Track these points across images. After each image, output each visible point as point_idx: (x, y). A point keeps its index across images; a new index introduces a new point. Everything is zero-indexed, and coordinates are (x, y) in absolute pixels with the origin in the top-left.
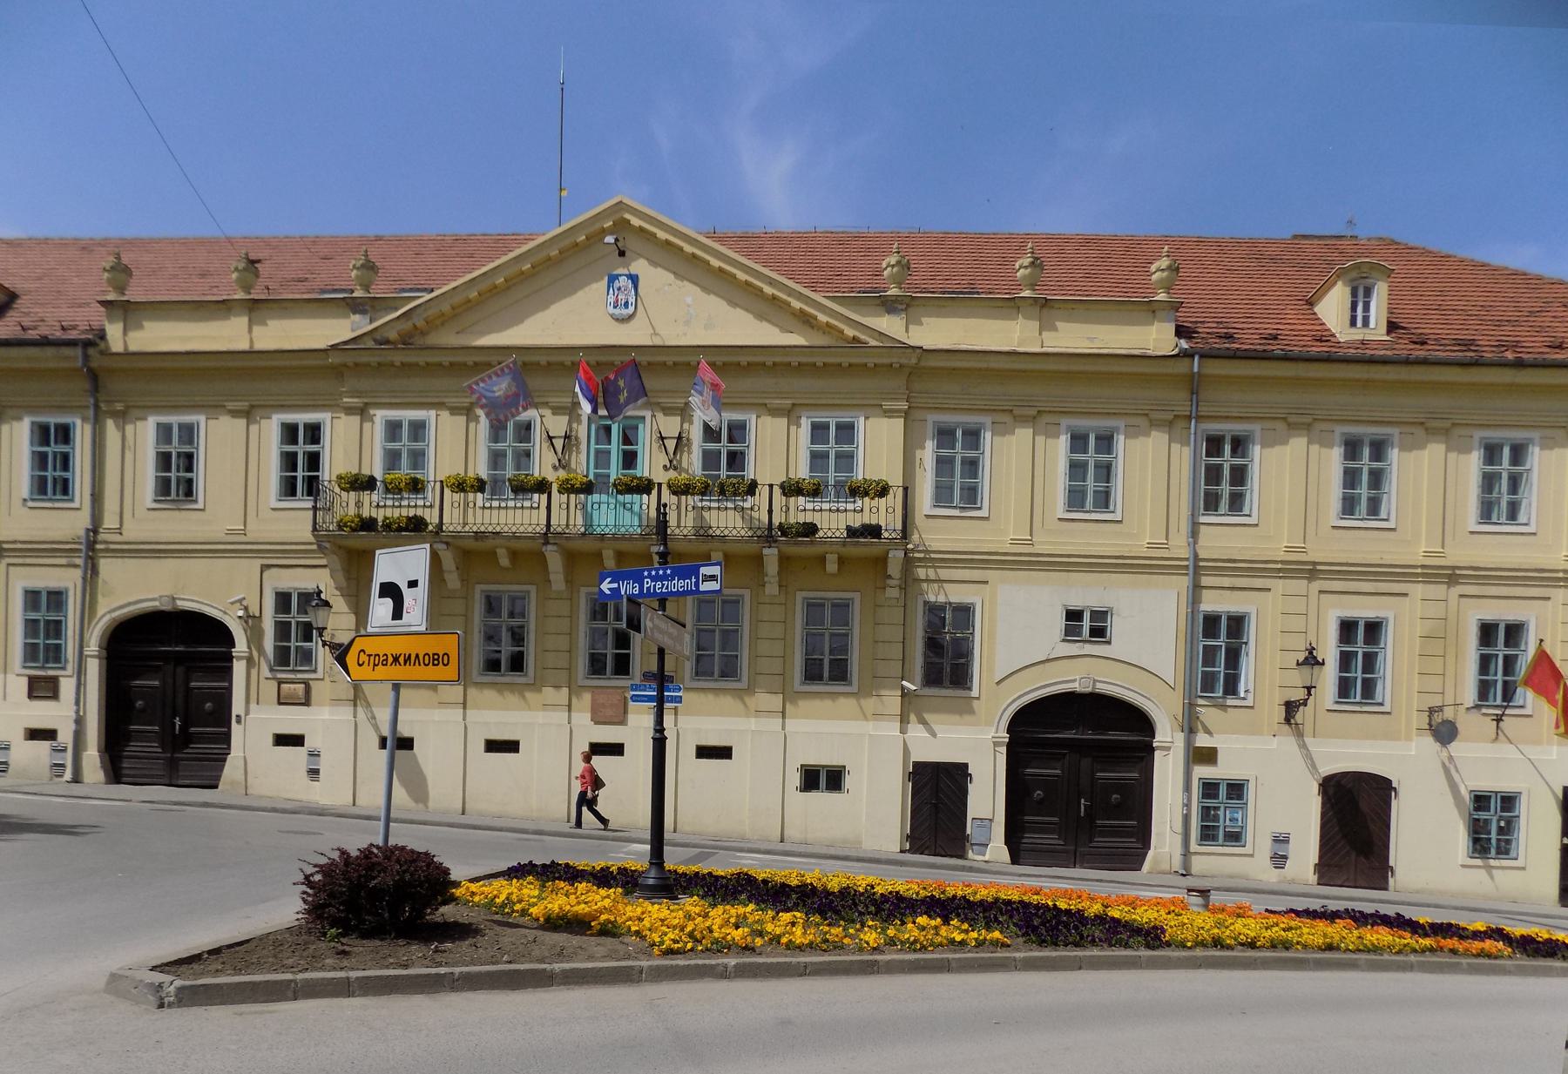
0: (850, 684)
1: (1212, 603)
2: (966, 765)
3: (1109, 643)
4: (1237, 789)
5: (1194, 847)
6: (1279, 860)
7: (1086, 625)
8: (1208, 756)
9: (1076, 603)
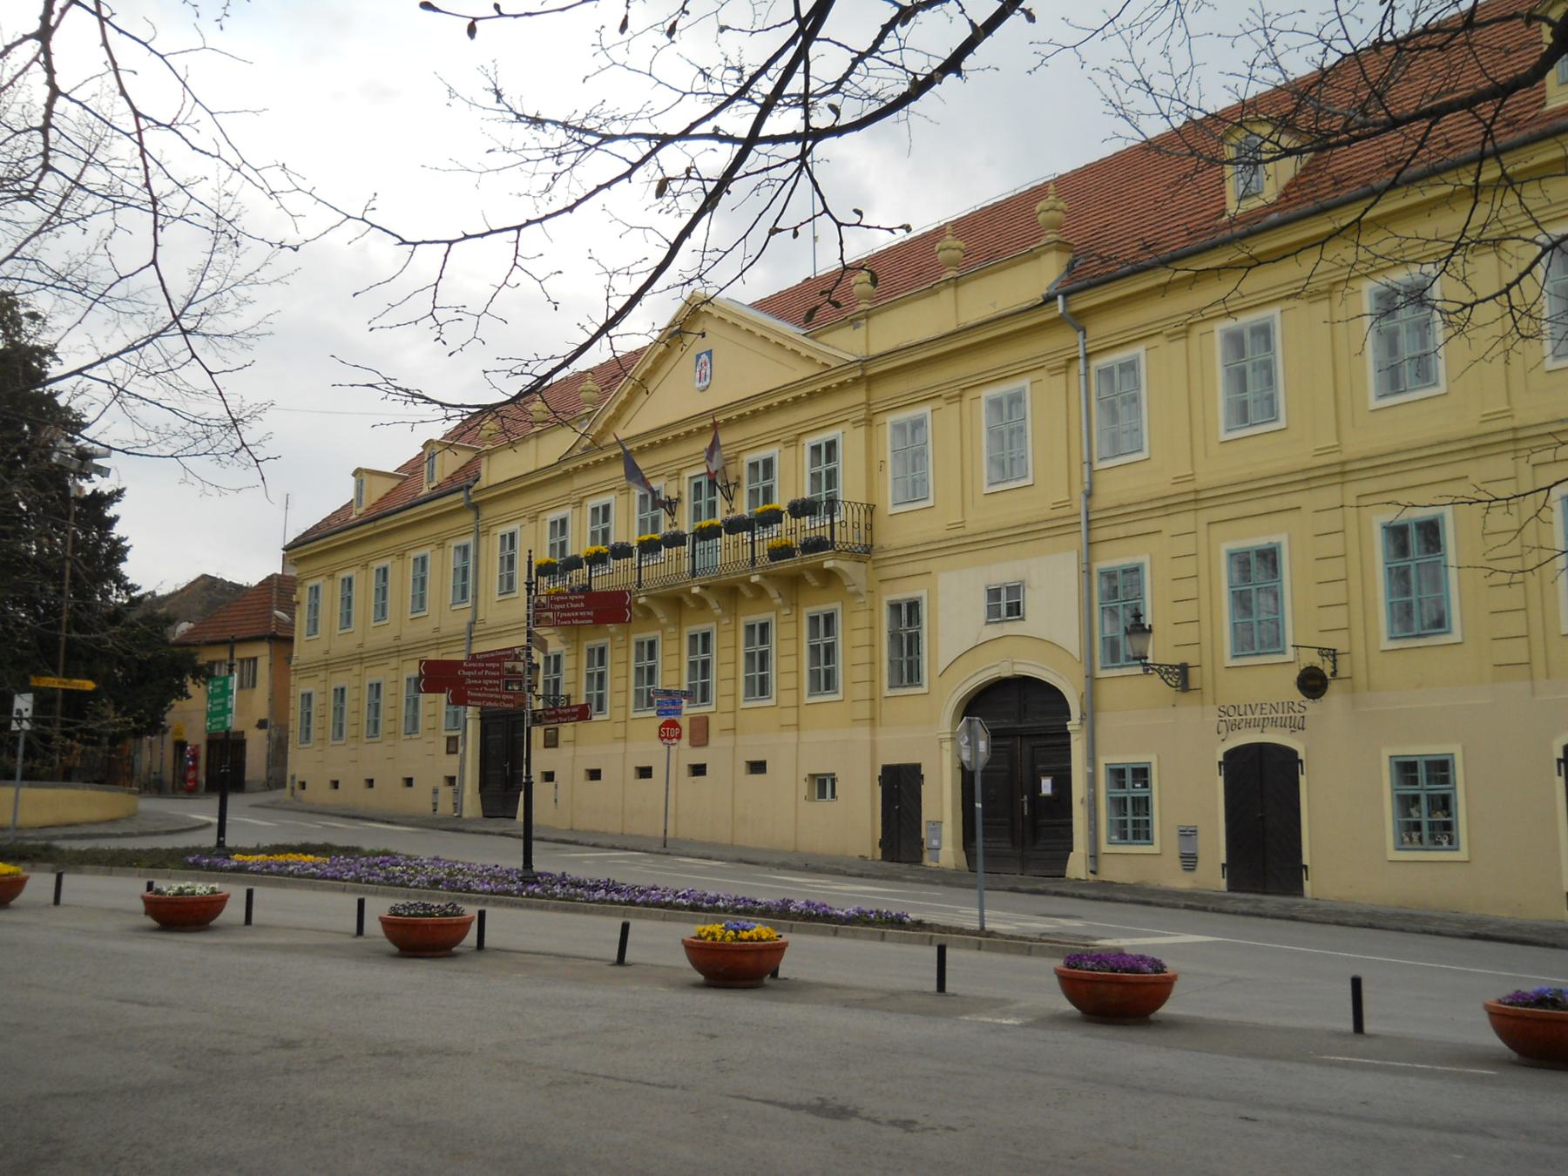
1: (1111, 558)
2: (917, 767)
5: (1104, 847)
6: (1189, 861)
7: (1007, 604)
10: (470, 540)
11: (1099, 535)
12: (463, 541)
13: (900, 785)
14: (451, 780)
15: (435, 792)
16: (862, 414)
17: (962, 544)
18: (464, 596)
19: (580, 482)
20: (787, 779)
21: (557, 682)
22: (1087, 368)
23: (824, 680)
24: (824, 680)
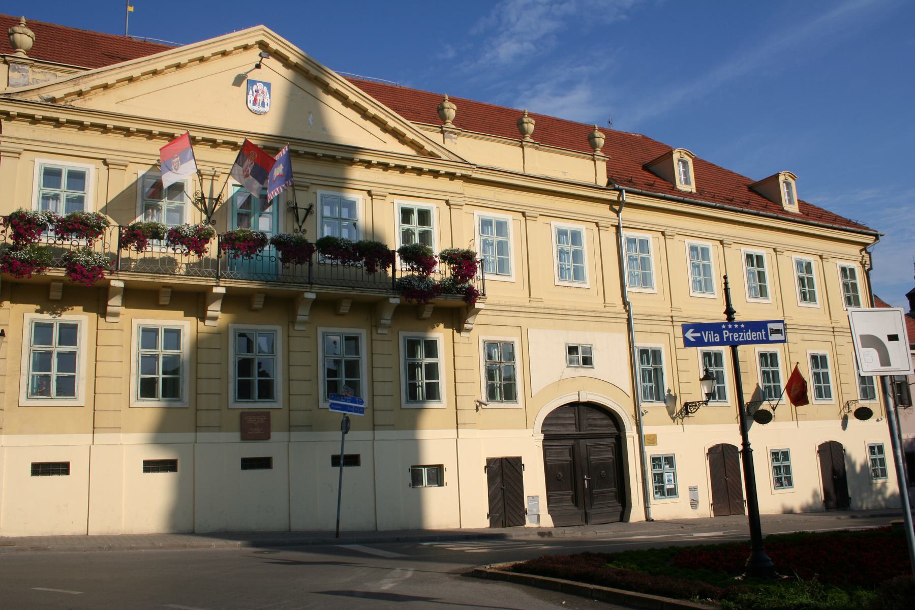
0: (407, 402)
4: (670, 460)
6: (694, 504)
8: (653, 440)
9: (573, 343)
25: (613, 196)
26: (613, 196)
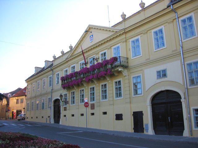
2: (142, 111)
3: (167, 77)
7: (162, 74)
9: (159, 70)
10: (52, 76)
11: (185, 56)
12: (50, 76)
13: (138, 117)
14: (49, 117)
15: (47, 119)
16: (125, 40)
17: (149, 63)
18: (51, 85)
19: (69, 63)
20: (112, 115)
21: (66, 99)
22: (178, 20)
23: (119, 95)
24: (119, 95)
25: (169, 9)
26: (169, 9)
